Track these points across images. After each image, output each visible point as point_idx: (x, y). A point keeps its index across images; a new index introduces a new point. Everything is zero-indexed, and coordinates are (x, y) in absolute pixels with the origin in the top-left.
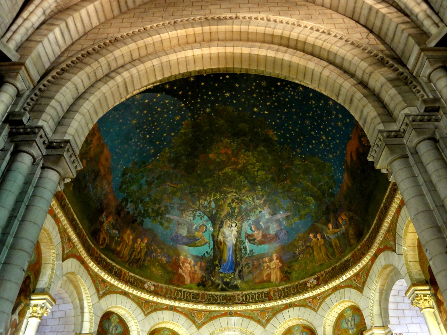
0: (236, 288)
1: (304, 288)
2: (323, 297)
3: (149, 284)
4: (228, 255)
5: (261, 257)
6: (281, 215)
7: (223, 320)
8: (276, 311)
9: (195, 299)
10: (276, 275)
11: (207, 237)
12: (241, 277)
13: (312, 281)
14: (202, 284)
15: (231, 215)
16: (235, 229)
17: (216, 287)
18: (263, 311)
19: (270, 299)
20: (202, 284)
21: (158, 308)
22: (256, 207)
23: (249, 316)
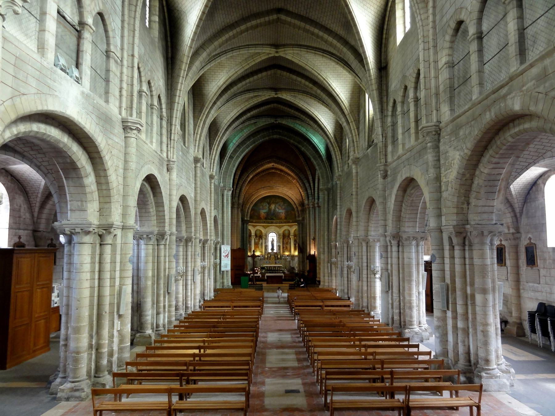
0: (274, 219)
1: (289, 222)
2: (293, 225)
3: (254, 221)
4: (272, 211)
5: (280, 213)
6: (286, 205)
7: (271, 227)
8: (283, 226)
9: (264, 223)
10: (283, 218)
11: (267, 207)
12: (275, 217)
13: (291, 221)
14: (266, 219)
15: (273, 203)
16: (274, 206)
17: (269, 219)
18: (280, 226)
19: (282, 223)
20: (266, 219)
21: (257, 226)
22: (279, 202)
23: (277, 226)
